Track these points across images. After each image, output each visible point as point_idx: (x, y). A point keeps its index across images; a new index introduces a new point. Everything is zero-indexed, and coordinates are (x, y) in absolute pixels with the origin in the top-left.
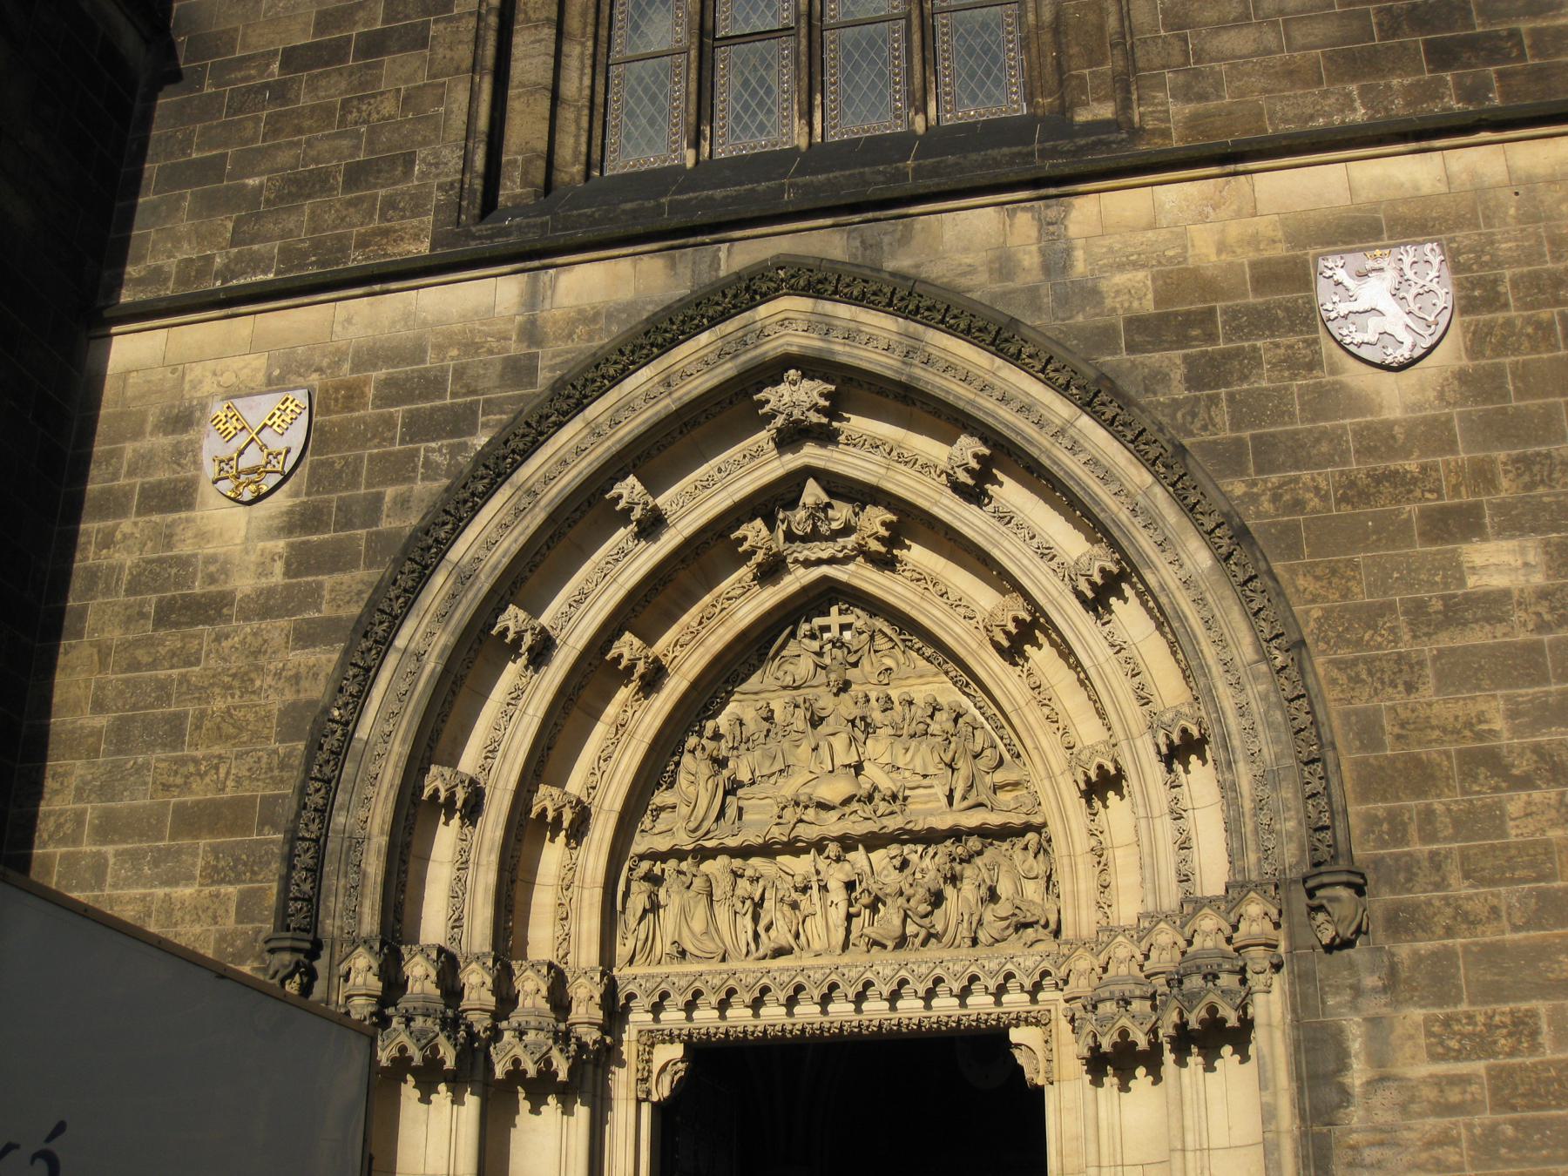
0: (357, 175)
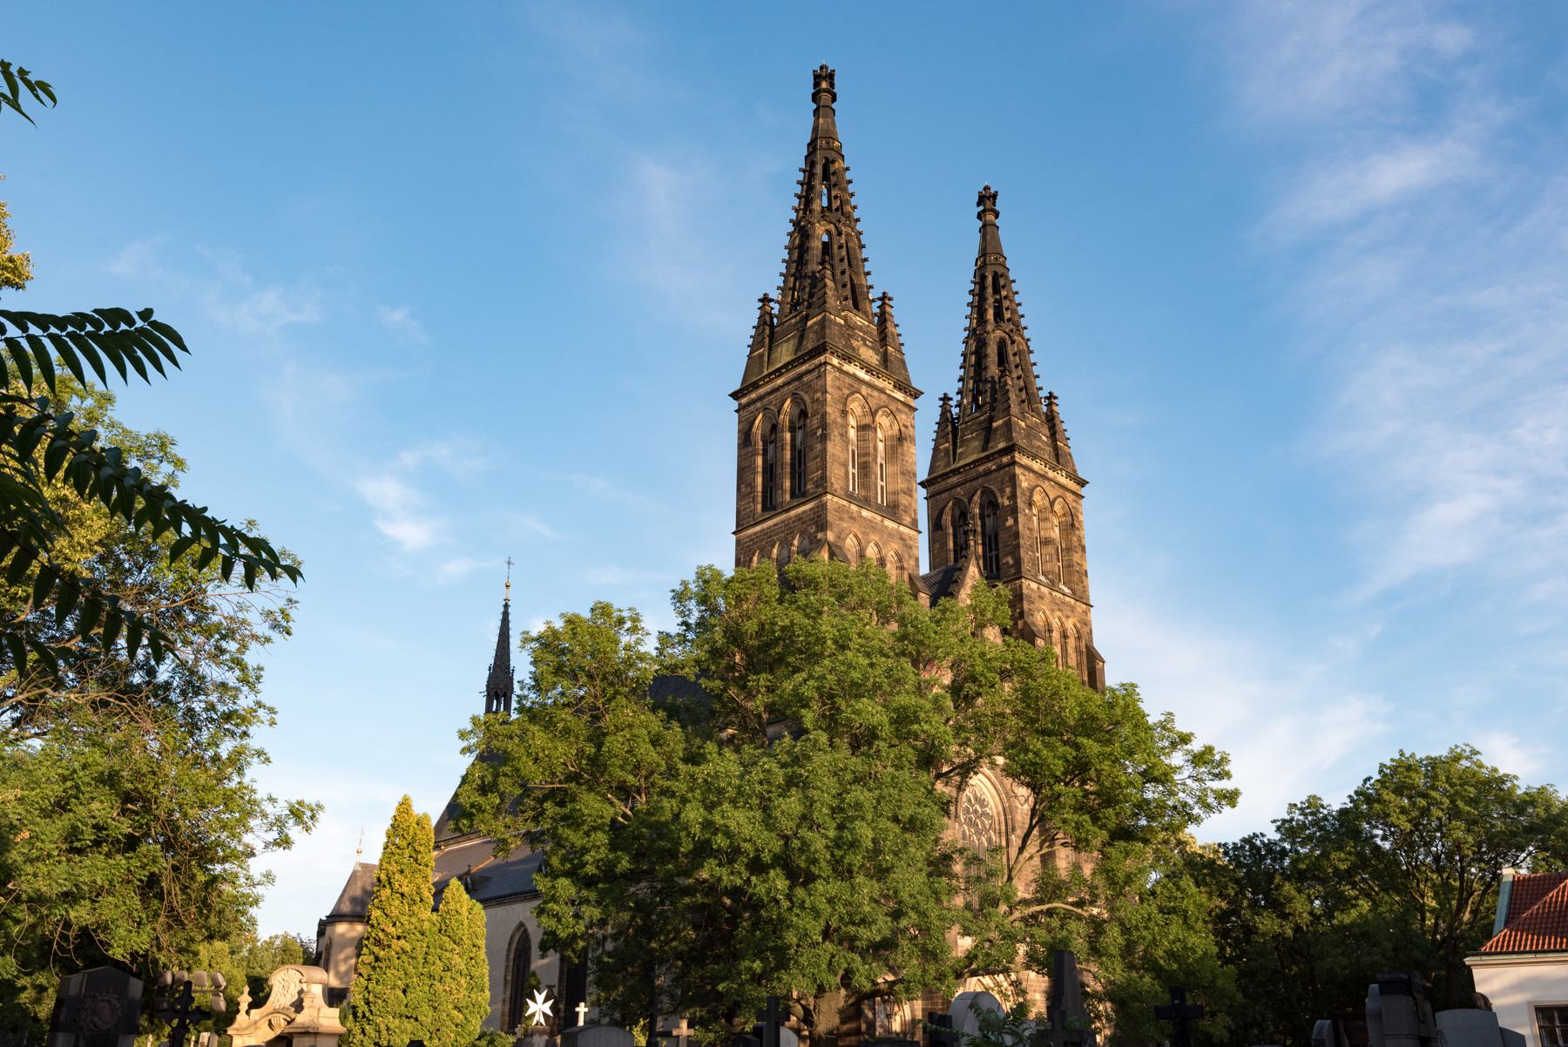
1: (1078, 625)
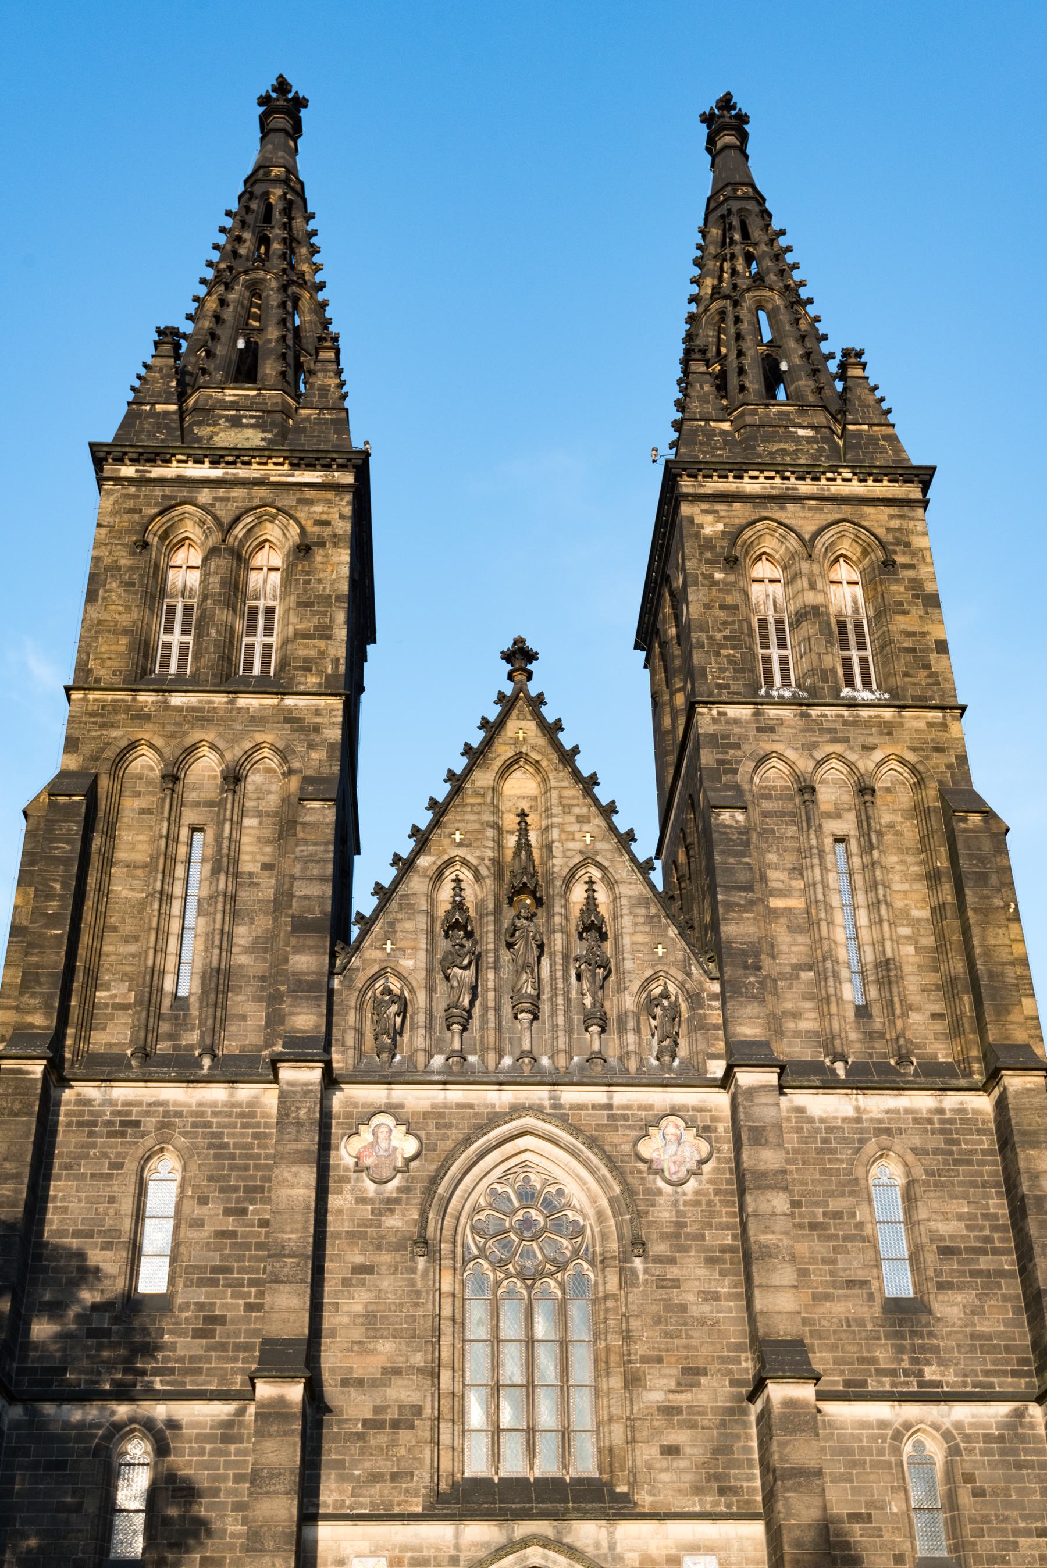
0: (395, 1477)
1: (911, 757)
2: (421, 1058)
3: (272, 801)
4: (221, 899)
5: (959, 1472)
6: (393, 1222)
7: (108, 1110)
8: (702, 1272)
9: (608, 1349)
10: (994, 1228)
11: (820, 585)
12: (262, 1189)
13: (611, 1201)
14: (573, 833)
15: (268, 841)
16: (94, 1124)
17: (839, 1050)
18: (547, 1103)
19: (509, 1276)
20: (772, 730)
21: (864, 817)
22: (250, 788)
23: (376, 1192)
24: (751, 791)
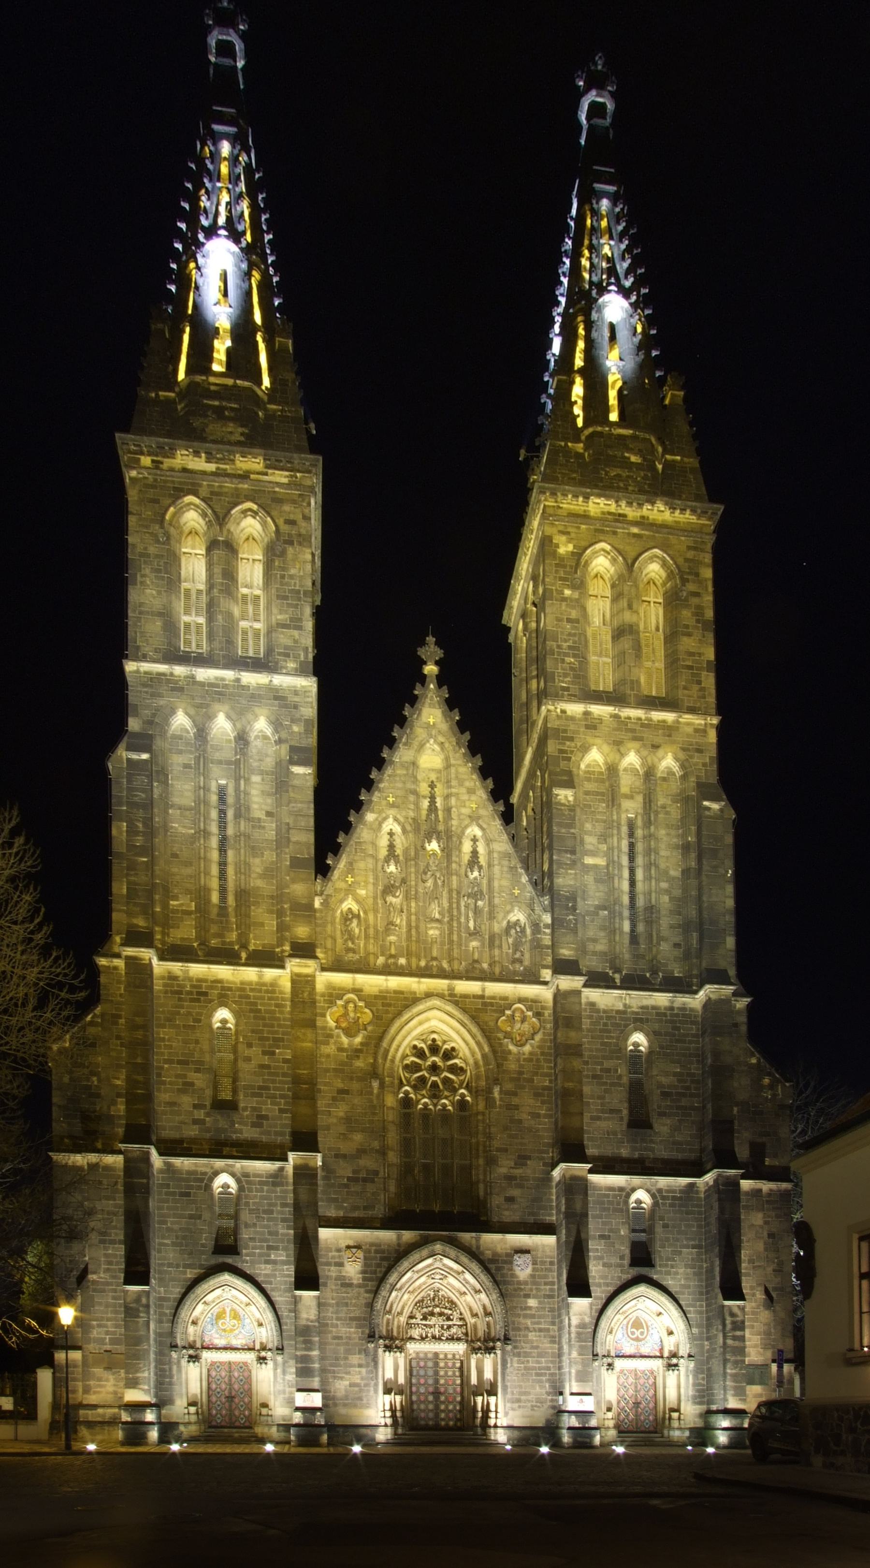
2: (372, 958)
3: (269, 763)
4: (242, 838)
5: (657, 1215)
6: (359, 1064)
7: (188, 984)
8: (531, 1101)
9: (478, 1143)
10: (692, 1082)
11: (635, 606)
12: (282, 1040)
13: (484, 1056)
14: (464, 802)
15: (269, 795)
16: (180, 993)
17: (618, 966)
18: (446, 993)
19: (424, 1097)
20: (595, 727)
21: (647, 800)
22: (254, 751)
23: (348, 1044)
24: (578, 775)
